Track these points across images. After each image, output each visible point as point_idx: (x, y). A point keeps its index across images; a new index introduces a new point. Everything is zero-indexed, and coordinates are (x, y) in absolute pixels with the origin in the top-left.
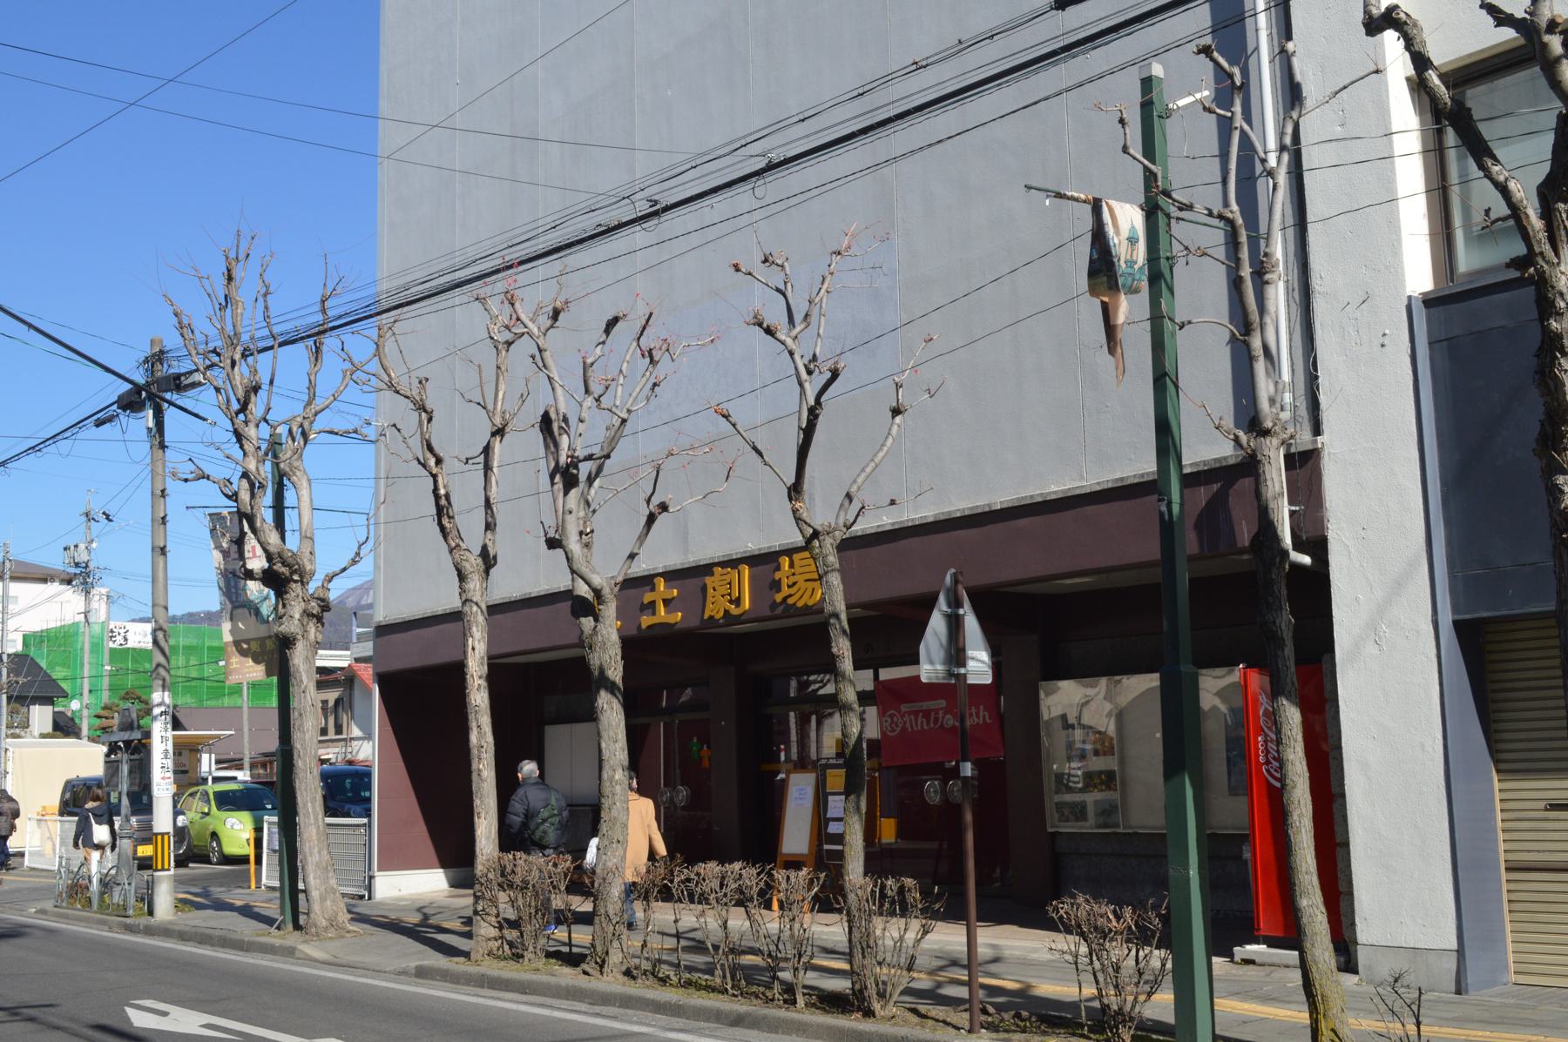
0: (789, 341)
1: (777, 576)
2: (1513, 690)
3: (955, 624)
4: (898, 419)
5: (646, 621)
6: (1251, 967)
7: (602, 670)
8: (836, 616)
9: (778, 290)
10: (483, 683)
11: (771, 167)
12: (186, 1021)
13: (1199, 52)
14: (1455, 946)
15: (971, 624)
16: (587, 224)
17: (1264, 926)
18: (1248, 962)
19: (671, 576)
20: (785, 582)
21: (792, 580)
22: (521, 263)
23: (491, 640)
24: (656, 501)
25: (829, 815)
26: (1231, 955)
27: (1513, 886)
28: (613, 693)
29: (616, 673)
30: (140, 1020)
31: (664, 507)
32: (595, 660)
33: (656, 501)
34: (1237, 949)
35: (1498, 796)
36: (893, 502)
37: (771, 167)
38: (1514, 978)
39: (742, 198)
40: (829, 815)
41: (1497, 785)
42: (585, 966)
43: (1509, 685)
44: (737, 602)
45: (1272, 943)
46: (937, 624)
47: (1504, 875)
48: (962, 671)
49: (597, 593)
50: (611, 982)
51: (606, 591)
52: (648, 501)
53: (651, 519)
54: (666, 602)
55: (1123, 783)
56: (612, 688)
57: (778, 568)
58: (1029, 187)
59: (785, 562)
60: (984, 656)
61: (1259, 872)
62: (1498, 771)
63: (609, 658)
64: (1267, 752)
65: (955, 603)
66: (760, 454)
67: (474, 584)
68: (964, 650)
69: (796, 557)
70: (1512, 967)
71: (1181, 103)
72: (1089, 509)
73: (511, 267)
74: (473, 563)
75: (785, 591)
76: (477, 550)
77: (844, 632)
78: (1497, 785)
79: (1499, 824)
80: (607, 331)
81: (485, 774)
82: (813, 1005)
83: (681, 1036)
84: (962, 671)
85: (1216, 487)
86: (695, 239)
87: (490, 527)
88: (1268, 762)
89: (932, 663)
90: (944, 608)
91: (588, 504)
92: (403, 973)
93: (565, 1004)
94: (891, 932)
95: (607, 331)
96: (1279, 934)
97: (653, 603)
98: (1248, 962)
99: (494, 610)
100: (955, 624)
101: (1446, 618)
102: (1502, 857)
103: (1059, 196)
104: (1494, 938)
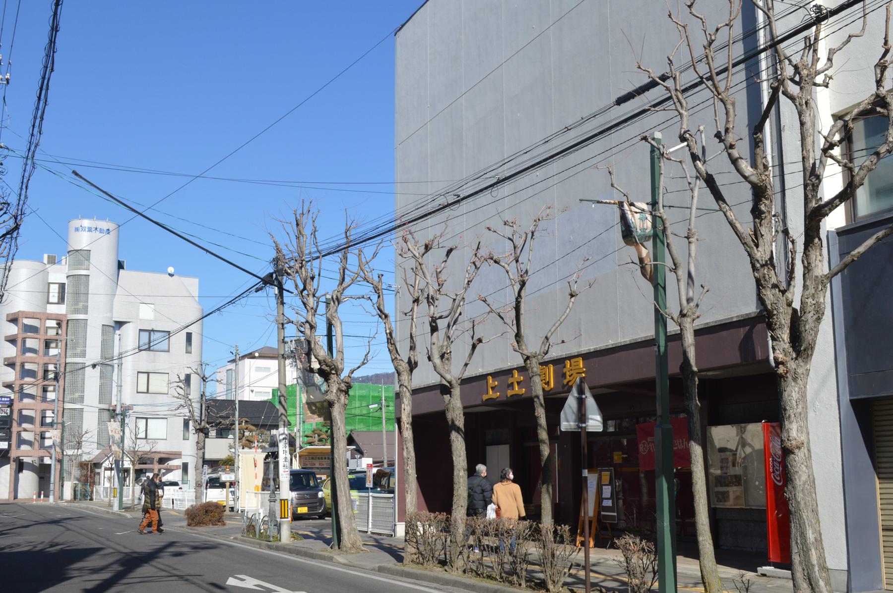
0: (506, 266)
1: (565, 370)
2: (886, 436)
3: (581, 402)
4: (573, 299)
5: (510, 393)
6: (764, 578)
7: (453, 421)
8: (537, 397)
9: (509, 239)
10: (409, 426)
11: (500, 182)
12: (250, 583)
13: (642, 139)
14: (846, 568)
15: (590, 402)
16: (435, 205)
17: (773, 557)
18: (764, 575)
19: (495, 375)
20: (568, 373)
21: (571, 372)
22: (410, 222)
23: (414, 405)
24: (476, 338)
25: (604, 496)
26: (756, 571)
27: (886, 539)
28: (458, 433)
29: (460, 422)
30: (231, 582)
31: (480, 341)
32: (449, 416)
33: (476, 338)
34: (759, 569)
35: (878, 491)
36: (563, 342)
37: (500, 182)
38: (886, 587)
39: (538, 174)
40: (604, 496)
41: (878, 486)
42: (446, 567)
43: (883, 433)
44: (548, 383)
45: (776, 566)
46: (571, 402)
47: (881, 533)
48: (584, 425)
49: (450, 383)
50: (454, 574)
51: (454, 382)
52: (473, 338)
53: (474, 347)
54: (518, 383)
55: (745, 481)
56: (458, 430)
57: (565, 367)
58: (581, 200)
59: (568, 363)
60: (599, 418)
61: (761, 530)
62: (879, 478)
63: (457, 416)
64: (774, 467)
65: (581, 391)
66: (502, 318)
67: (405, 377)
68: (585, 415)
69: (573, 361)
70: (885, 581)
71: (672, 150)
72: (724, 333)
73: (404, 224)
74: (404, 366)
75: (568, 378)
76: (406, 360)
77: (541, 405)
78: (878, 486)
79: (879, 506)
80: (447, 255)
81: (410, 472)
82: (531, 587)
83: (431, 591)
84: (584, 425)
85: (747, 328)
86: (530, 192)
87: (412, 348)
88: (774, 472)
89: (568, 421)
90: (576, 395)
91: (449, 338)
92: (373, 569)
93: (404, 579)
94: (562, 550)
95: (447, 255)
96: (779, 561)
97: (512, 383)
98: (764, 575)
99: (415, 392)
100: (581, 402)
101: (846, 398)
102: (880, 523)
103: (598, 202)
104: (872, 565)
